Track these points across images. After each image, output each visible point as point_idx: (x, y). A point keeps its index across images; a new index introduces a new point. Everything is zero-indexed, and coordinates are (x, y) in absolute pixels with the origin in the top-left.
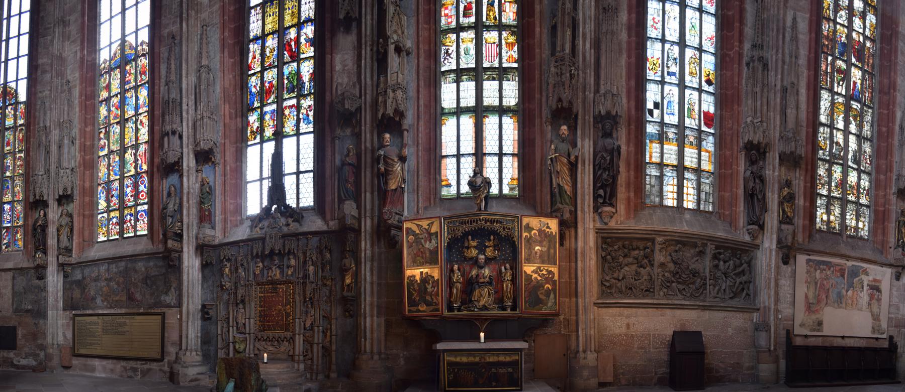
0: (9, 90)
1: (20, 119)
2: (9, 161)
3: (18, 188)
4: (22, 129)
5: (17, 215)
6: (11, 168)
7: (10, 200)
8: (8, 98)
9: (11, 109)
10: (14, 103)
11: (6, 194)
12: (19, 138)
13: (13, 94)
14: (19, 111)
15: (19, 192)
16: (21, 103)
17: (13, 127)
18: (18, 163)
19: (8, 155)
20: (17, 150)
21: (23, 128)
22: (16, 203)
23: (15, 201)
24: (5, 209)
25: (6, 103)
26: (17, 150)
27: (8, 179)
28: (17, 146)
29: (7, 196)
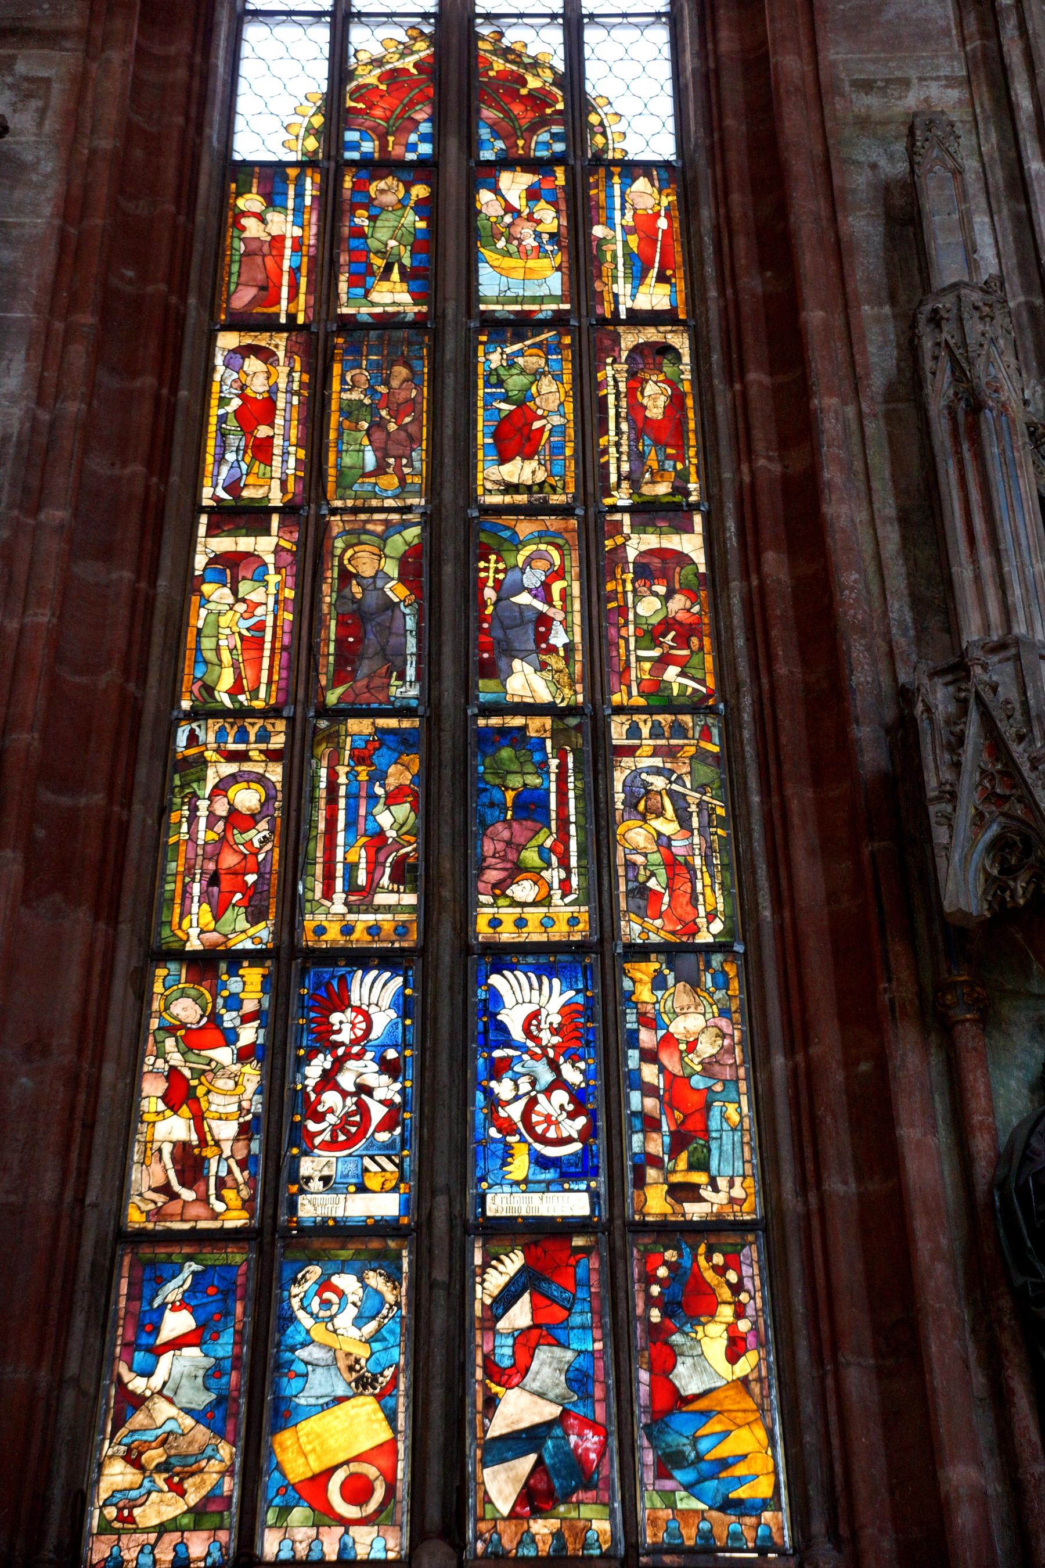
0: (499, 64)
1: (638, 278)
2: (533, 578)
3: (668, 827)
4: (665, 350)
5: (669, 1103)
6: (558, 638)
7: (559, 932)
8: (489, 113)
9: (533, 194)
10: (558, 160)
11: (517, 871)
12: (636, 409)
13: (538, 100)
14: (623, 219)
15: (672, 864)
16: (632, 169)
17: (558, 321)
18: (649, 608)
19: (525, 528)
20: (622, 498)
21: (681, 342)
22: (643, 972)
23: (641, 952)
24: (513, 1018)
25: (471, 144)
26: (622, 498)
27: (538, 726)
28: (617, 464)
29: (524, 890)
